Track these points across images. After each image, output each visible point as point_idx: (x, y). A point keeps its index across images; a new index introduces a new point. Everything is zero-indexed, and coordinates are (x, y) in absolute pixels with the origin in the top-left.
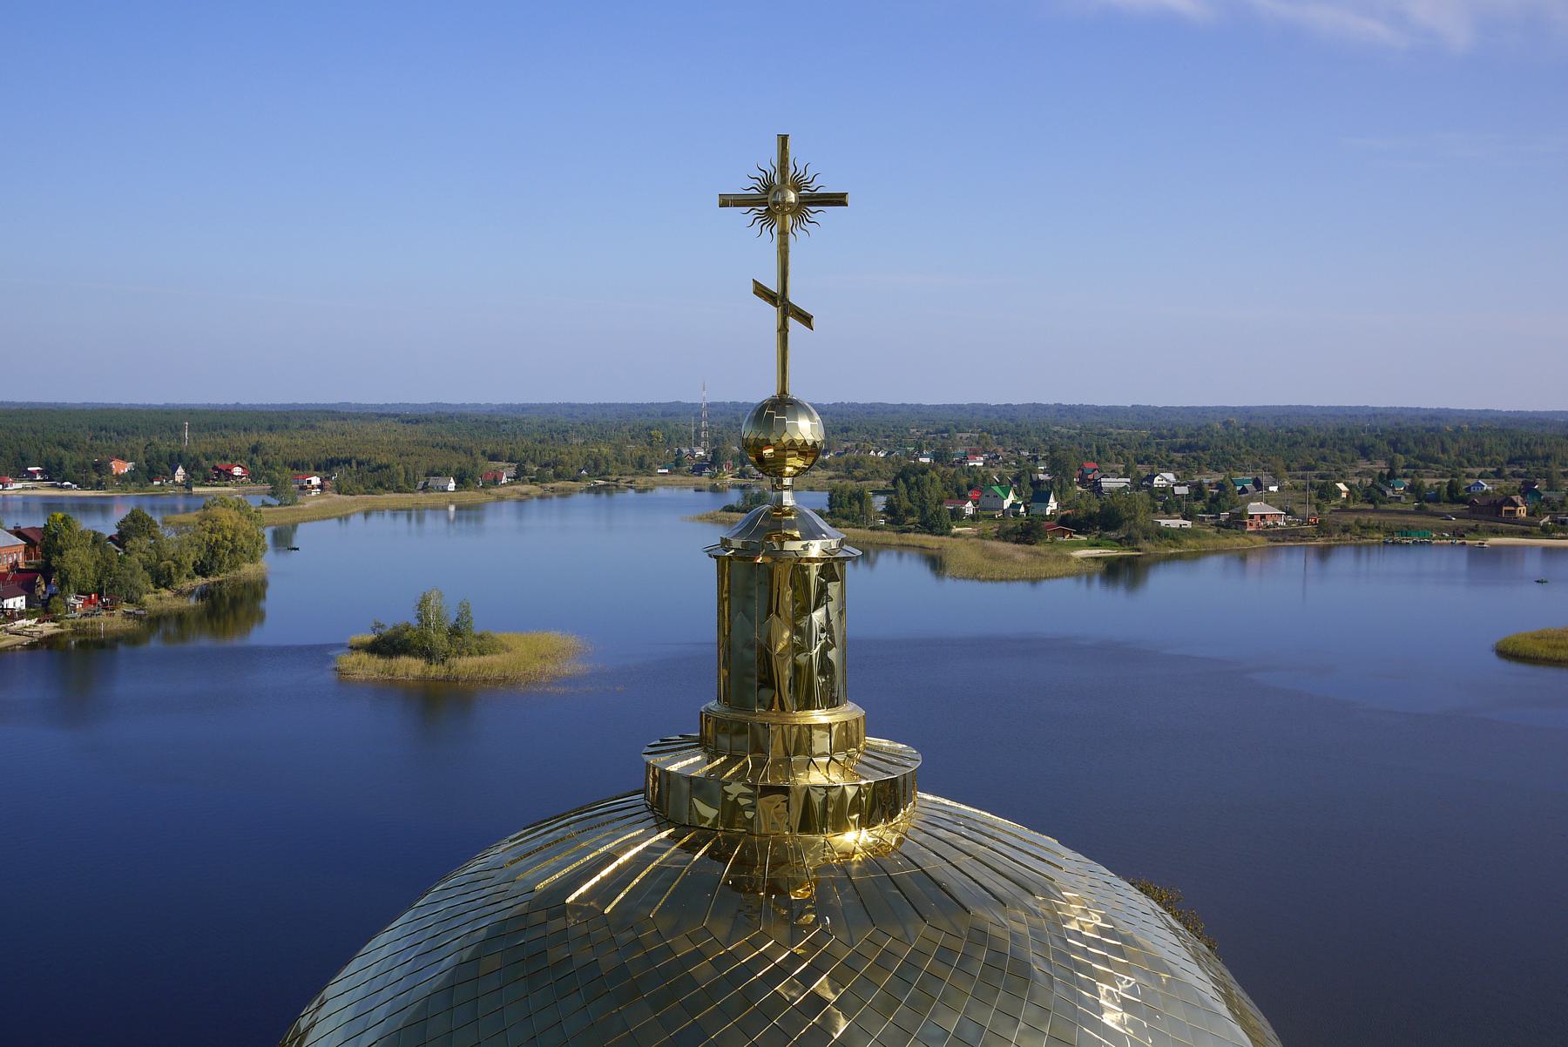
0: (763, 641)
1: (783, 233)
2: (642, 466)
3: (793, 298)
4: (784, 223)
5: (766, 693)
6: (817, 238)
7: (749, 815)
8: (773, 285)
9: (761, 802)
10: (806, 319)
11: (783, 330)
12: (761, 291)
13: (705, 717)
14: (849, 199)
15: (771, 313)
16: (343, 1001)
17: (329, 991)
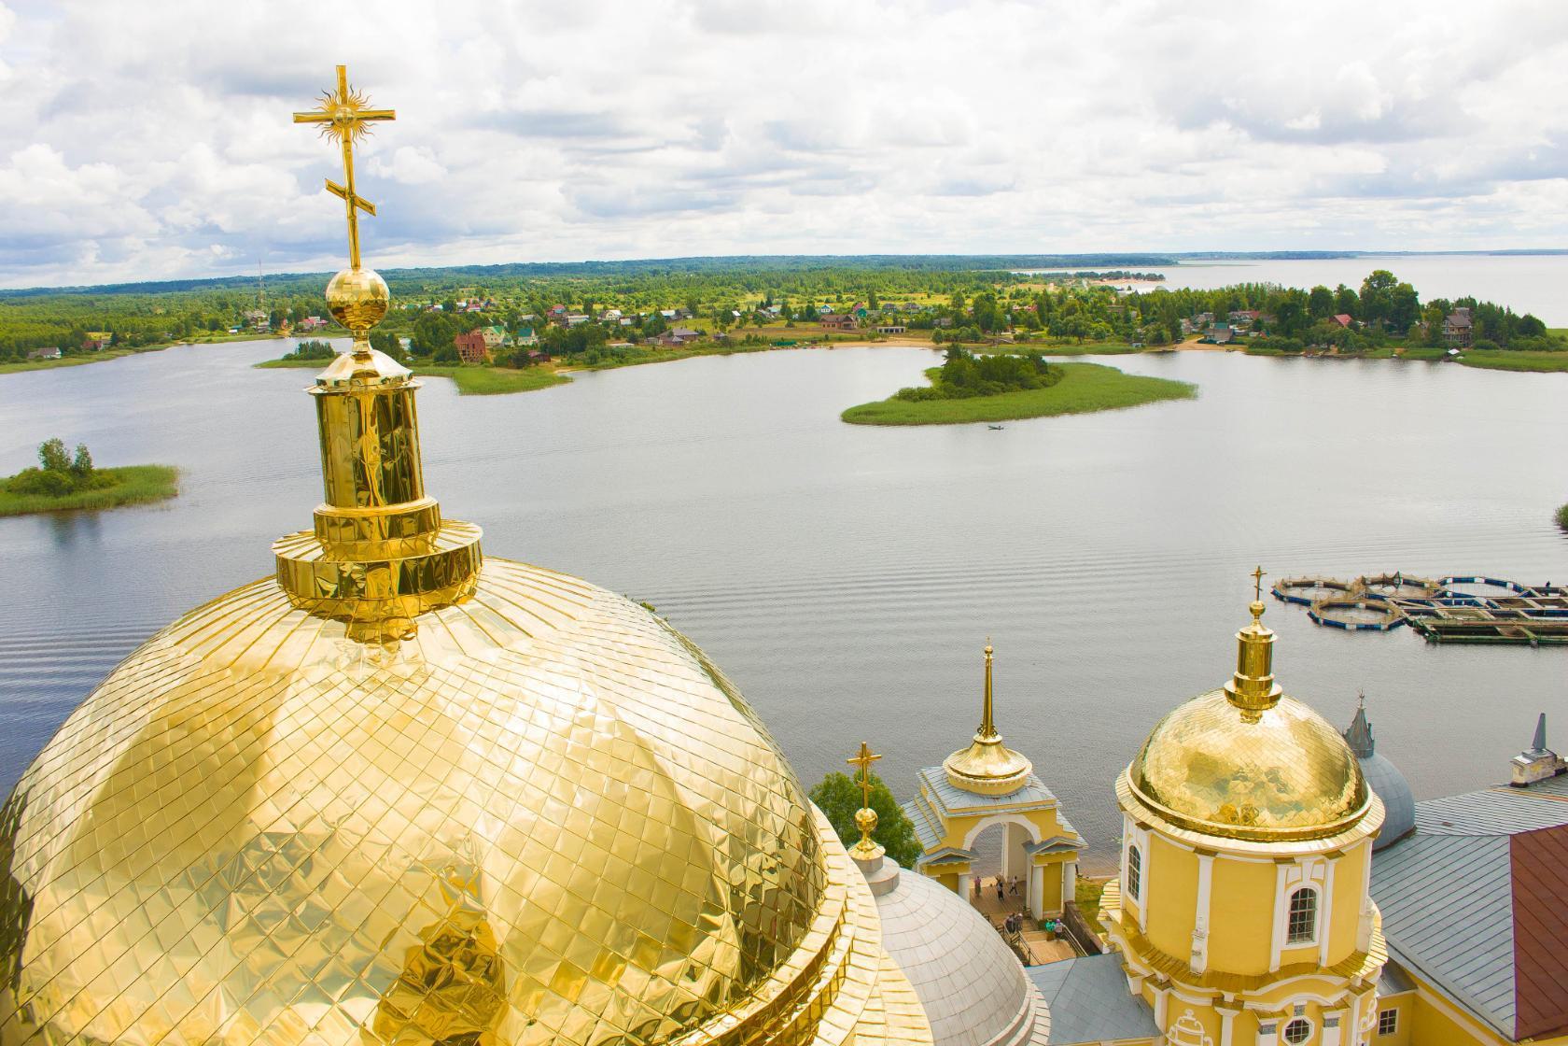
0: (357, 455)
1: (346, 141)
2: (215, 326)
3: (358, 192)
4: (347, 134)
5: (363, 494)
6: (370, 141)
7: (361, 585)
8: (344, 185)
9: (369, 576)
10: (370, 209)
11: (353, 218)
12: (331, 188)
13: (319, 518)
14: (397, 116)
15: (341, 204)
16: (60, 761)
17: (45, 757)
